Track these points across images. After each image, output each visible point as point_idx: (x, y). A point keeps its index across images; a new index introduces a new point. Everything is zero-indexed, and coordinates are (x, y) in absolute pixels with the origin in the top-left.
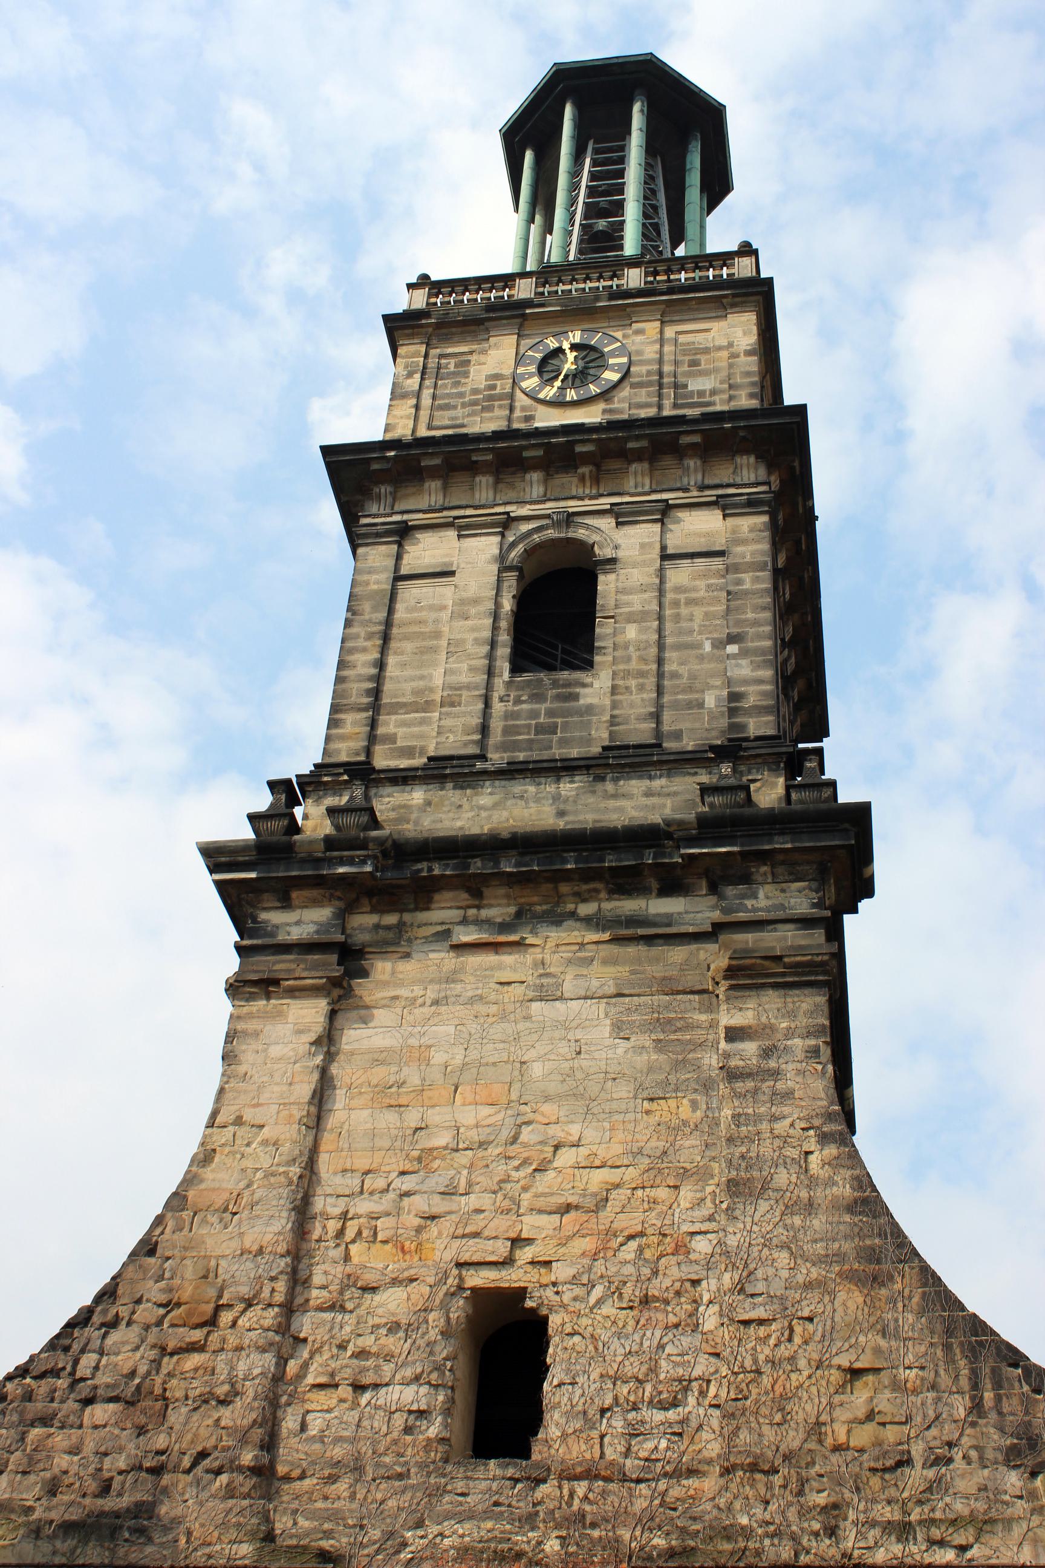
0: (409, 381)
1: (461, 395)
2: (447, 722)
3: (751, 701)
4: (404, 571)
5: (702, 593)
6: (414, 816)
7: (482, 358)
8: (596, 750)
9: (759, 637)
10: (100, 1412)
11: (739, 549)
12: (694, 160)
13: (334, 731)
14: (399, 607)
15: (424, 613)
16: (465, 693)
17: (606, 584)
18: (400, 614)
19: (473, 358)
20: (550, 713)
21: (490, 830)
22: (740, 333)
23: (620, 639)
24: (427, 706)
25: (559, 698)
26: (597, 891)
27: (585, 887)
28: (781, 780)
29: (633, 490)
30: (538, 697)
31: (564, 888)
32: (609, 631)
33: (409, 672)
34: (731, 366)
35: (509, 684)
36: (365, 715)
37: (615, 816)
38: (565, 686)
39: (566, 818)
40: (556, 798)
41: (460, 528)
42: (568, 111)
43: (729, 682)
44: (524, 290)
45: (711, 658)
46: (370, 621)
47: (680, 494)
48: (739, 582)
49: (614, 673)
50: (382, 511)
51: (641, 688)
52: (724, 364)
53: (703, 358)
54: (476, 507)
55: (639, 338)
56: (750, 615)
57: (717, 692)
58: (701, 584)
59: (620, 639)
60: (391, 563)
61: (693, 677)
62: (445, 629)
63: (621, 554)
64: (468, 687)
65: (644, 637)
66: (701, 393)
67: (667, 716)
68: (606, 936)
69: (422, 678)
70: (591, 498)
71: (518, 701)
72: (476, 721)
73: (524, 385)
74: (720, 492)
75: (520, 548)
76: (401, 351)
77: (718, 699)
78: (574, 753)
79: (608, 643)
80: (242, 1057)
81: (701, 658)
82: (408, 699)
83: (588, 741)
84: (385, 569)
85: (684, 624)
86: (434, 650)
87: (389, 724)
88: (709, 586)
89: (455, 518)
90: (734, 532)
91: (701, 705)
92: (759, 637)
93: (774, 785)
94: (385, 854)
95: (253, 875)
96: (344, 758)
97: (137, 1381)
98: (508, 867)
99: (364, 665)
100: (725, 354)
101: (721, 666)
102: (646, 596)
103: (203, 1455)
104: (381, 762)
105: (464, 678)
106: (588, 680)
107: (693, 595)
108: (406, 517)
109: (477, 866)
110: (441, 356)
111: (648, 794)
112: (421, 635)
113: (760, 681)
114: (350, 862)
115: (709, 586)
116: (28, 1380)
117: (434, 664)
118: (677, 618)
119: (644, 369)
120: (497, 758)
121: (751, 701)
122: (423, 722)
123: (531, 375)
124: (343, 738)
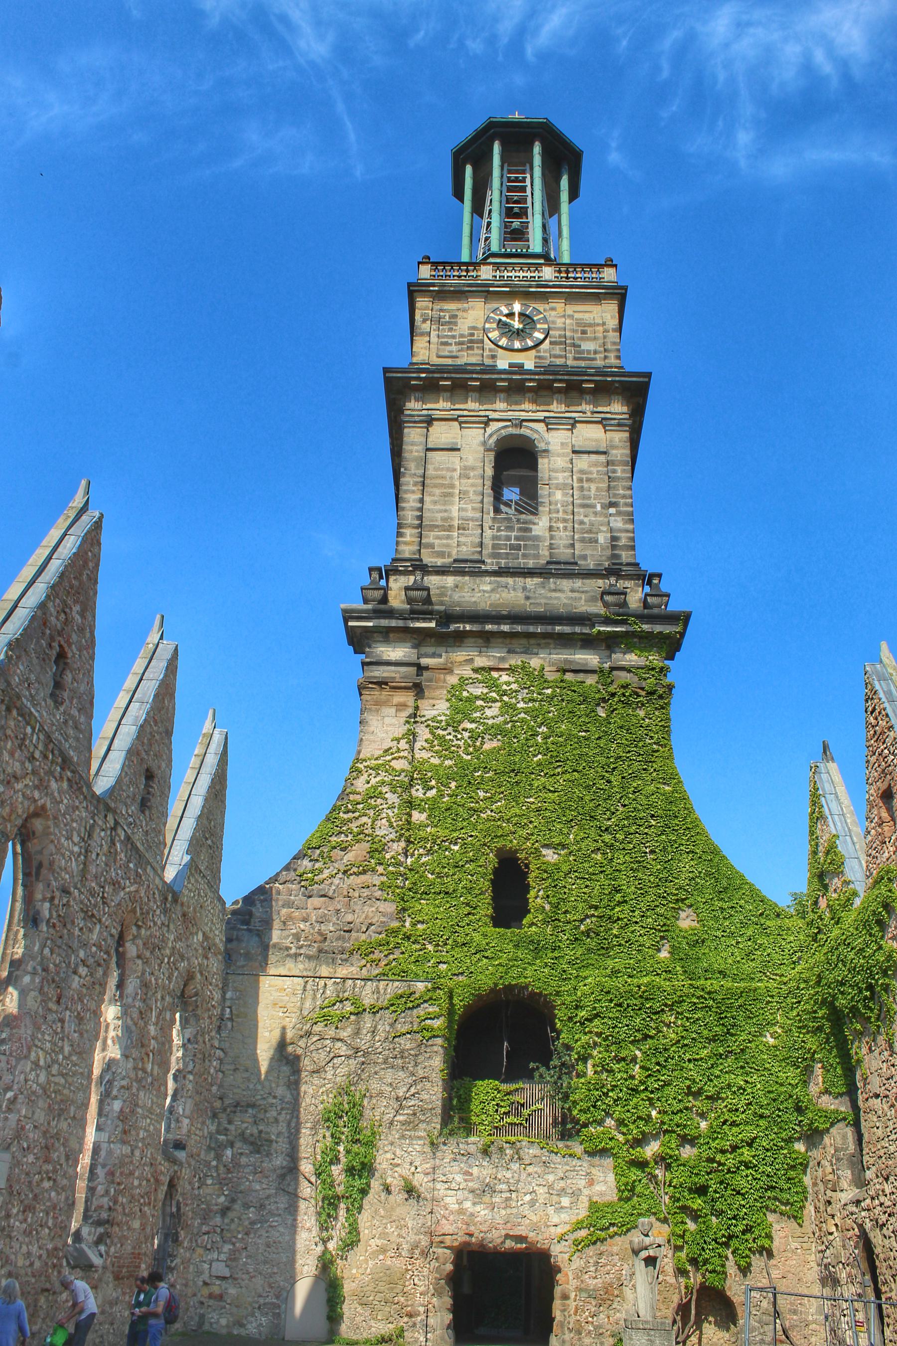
0: (424, 326)
1: (454, 337)
2: (462, 539)
3: (623, 542)
4: (429, 446)
5: (595, 475)
6: (449, 593)
7: (465, 315)
8: (543, 561)
9: (626, 505)
10: (316, 901)
11: (614, 452)
12: (564, 183)
13: (400, 539)
14: (429, 466)
15: (444, 472)
16: (471, 523)
17: (543, 463)
18: (430, 472)
19: (460, 314)
20: (517, 538)
21: (491, 605)
22: (609, 317)
23: (552, 499)
24: (450, 528)
25: (520, 529)
26: (549, 644)
27: (544, 641)
28: (641, 589)
29: (555, 410)
30: (510, 528)
31: (532, 641)
32: (546, 493)
33: (438, 507)
34: (605, 337)
35: (494, 519)
36: (417, 531)
37: (556, 602)
38: (523, 523)
39: (531, 601)
40: (524, 589)
41: (461, 423)
42: (497, 148)
43: (611, 530)
44: (486, 273)
45: (601, 514)
46: (415, 474)
47: (581, 414)
48: (614, 471)
49: (551, 519)
50: (416, 407)
51: (565, 528)
52: (601, 335)
53: (589, 329)
54: (469, 411)
55: (553, 313)
56: (621, 492)
57: (605, 534)
58: (594, 470)
59: (552, 499)
60: (423, 439)
61: (592, 524)
62: (457, 483)
63: (551, 448)
64: (472, 520)
65: (565, 499)
66: (589, 352)
67: (577, 546)
68: (554, 669)
69: (446, 511)
70: (533, 412)
71: (499, 530)
72: (478, 540)
73: (490, 335)
74: (603, 415)
75: (495, 438)
76: (418, 305)
77: (605, 538)
78: (531, 563)
79: (546, 500)
80: (370, 722)
81: (595, 514)
82: (439, 523)
83: (537, 556)
84: (421, 443)
85: (586, 493)
86: (451, 495)
87: (430, 537)
88: (598, 471)
89: (459, 416)
90: (611, 441)
91: (596, 541)
92: (626, 505)
93: (637, 592)
94: (440, 617)
95: (371, 624)
96: (407, 555)
97: (334, 888)
98: (505, 628)
99: (414, 501)
100: (601, 329)
101: (606, 520)
102: (566, 474)
103: (371, 924)
104: (428, 559)
105: (470, 514)
106: (536, 521)
107: (590, 476)
108: (430, 412)
109: (489, 627)
110: (441, 310)
111: (572, 591)
112: (443, 486)
113: (627, 531)
114: (425, 620)
115: (598, 471)
116: (277, 885)
117: (452, 504)
118: (582, 489)
119: (557, 333)
120: (491, 564)
121: (623, 542)
122: (448, 537)
123: (494, 330)
124: (406, 543)
